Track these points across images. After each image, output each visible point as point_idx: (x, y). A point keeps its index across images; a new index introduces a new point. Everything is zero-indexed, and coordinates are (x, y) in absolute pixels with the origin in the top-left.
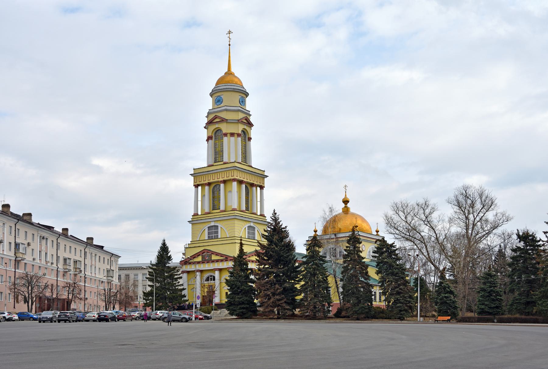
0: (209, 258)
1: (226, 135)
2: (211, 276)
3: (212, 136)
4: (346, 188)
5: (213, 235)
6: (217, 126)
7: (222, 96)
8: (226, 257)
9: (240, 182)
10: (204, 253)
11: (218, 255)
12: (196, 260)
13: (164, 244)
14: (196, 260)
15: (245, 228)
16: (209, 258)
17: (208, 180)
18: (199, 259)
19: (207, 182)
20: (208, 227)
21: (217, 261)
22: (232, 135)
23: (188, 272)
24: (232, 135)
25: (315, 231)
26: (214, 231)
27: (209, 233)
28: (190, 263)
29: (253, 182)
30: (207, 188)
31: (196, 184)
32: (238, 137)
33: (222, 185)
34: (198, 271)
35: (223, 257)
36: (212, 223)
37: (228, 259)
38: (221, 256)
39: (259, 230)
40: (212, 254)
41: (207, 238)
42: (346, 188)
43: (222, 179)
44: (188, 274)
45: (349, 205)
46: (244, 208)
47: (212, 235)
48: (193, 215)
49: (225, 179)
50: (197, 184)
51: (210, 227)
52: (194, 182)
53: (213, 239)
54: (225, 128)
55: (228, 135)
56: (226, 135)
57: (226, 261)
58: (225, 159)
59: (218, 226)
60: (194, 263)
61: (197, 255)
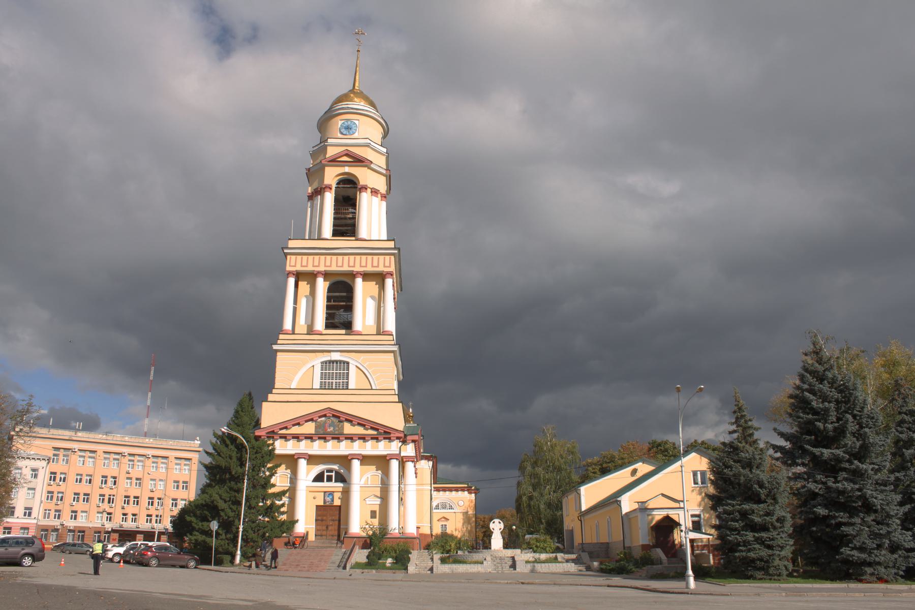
0: (337, 429)
1: (365, 188)
2: (328, 471)
5: (334, 381)
6: (347, 169)
7: (357, 122)
8: (385, 432)
10: (325, 416)
12: (295, 430)
14: (295, 430)
16: (337, 429)
17: (325, 266)
19: (322, 268)
20: (322, 363)
21: (363, 438)
22: (375, 192)
24: (375, 192)
27: (323, 376)
32: (381, 200)
33: (359, 283)
35: (377, 430)
36: (332, 354)
37: (392, 435)
38: (372, 428)
40: (347, 420)
41: (317, 385)
47: (331, 381)
49: (369, 269)
53: (332, 389)
54: (363, 175)
55: (369, 190)
56: (365, 188)
57: (385, 438)
58: (363, 232)
59: (348, 363)
60: (297, 437)
61: (309, 418)
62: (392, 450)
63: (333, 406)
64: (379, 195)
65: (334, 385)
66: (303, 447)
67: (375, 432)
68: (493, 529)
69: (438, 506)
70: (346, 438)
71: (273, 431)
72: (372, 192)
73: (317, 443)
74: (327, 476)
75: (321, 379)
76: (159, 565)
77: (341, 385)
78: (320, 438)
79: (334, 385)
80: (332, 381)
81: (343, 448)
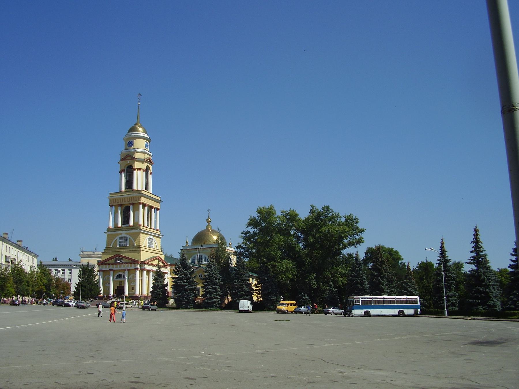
1: (135, 169)
3: (125, 170)
4: (209, 211)
5: (123, 244)
8: (134, 261)
9: (144, 205)
12: (109, 262)
14: (109, 262)
17: (121, 202)
18: (113, 261)
19: (120, 203)
21: (127, 263)
22: (139, 169)
23: (104, 271)
24: (139, 169)
25: (187, 242)
28: (105, 264)
29: (153, 205)
31: (111, 204)
33: (131, 207)
42: (209, 211)
43: (132, 202)
44: (103, 273)
46: (146, 225)
50: (112, 205)
52: (110, 203)
58: (135, 188)
60: (109, 264)
61: (111, 258)
64: (142, 170)
66: (111, 267)
67: (132, 261)
73: (115, 266)
76: (104, 308)
81: (122, 267)
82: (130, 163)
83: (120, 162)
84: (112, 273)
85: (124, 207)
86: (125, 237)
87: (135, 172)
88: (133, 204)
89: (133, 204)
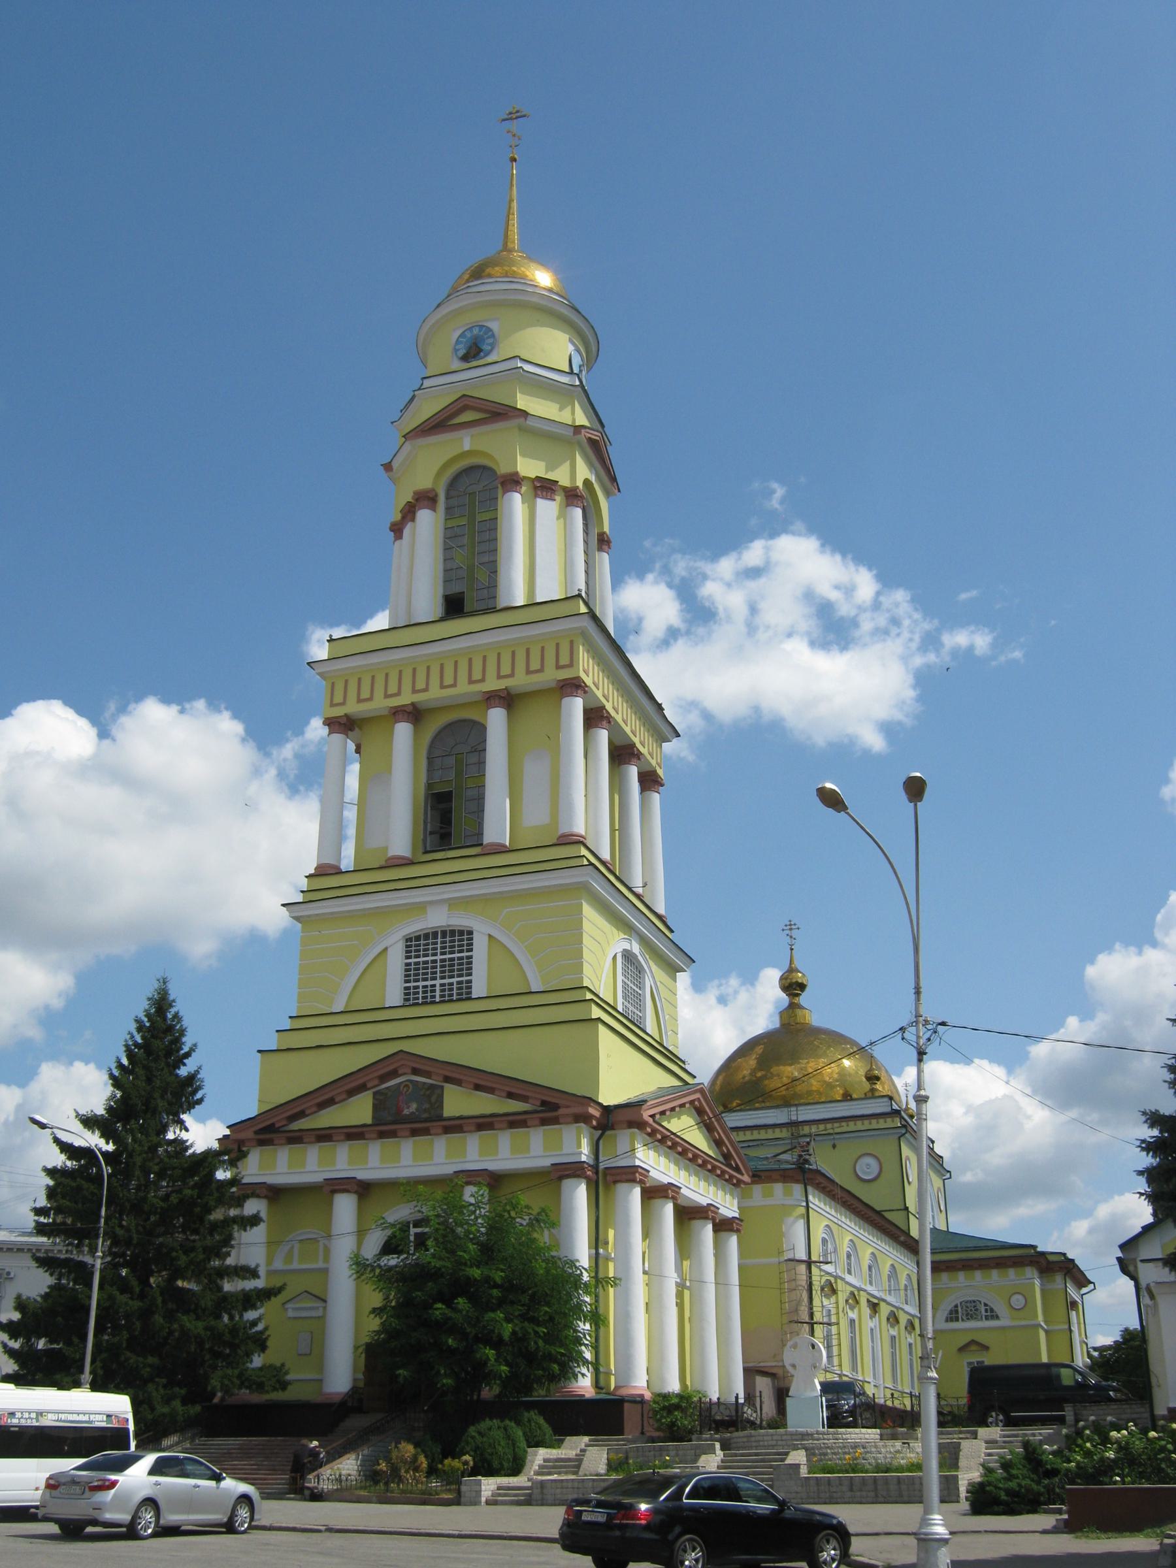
0: (427, 1106)
4: (795, 933)
5: (438, 982)
8: (544, 1103)
10: (394, 1074)
11: (490, 1090)
13: (161, 1003)
15: (615, 958)
17: (414, 691)
18: (359, 1110)
20: (408, 940)
21: (484, 1123)
22: (544, 487)
24: (544, 487)
26: (443, 961)
27: (410, 973)
28: (296, 1139)
30: (403, 731)
31: (339, 712)
32: (568, 505)
34: (336, 1186)
37: (561, 1111)
38: (510, 1095)
39: (659, 994)
40: (448, 1079)
41: (394, 995)
42: (795, 933)
45: (804, 999)
47: (429, 983)
48: (313, 871)
50: (346, 715)
51: (418, 938)
53: (434, 1003)
57: (544, 1122)
59: (470, 933)
60: (324, 1136)
62: (565, 1151)
63: (407, 1046)
65: (438, 993)
68: (794, 1366)
69: (957, 1312)
70: (447, 1130)
71: (273, 1125)
72: (536, 488)
74: (416, 1235)
75: (406, 982)
77: (455, 992)
78: (382, 1135)
79: (438, 993)
80: (433, 982)
82: (475, 448)
83: (395, 465)
84: (345, 1207)
85: (432, 726)
86: (453, 933)
87: (516, 504)
88: (508, 700)
89: (508, 700)
